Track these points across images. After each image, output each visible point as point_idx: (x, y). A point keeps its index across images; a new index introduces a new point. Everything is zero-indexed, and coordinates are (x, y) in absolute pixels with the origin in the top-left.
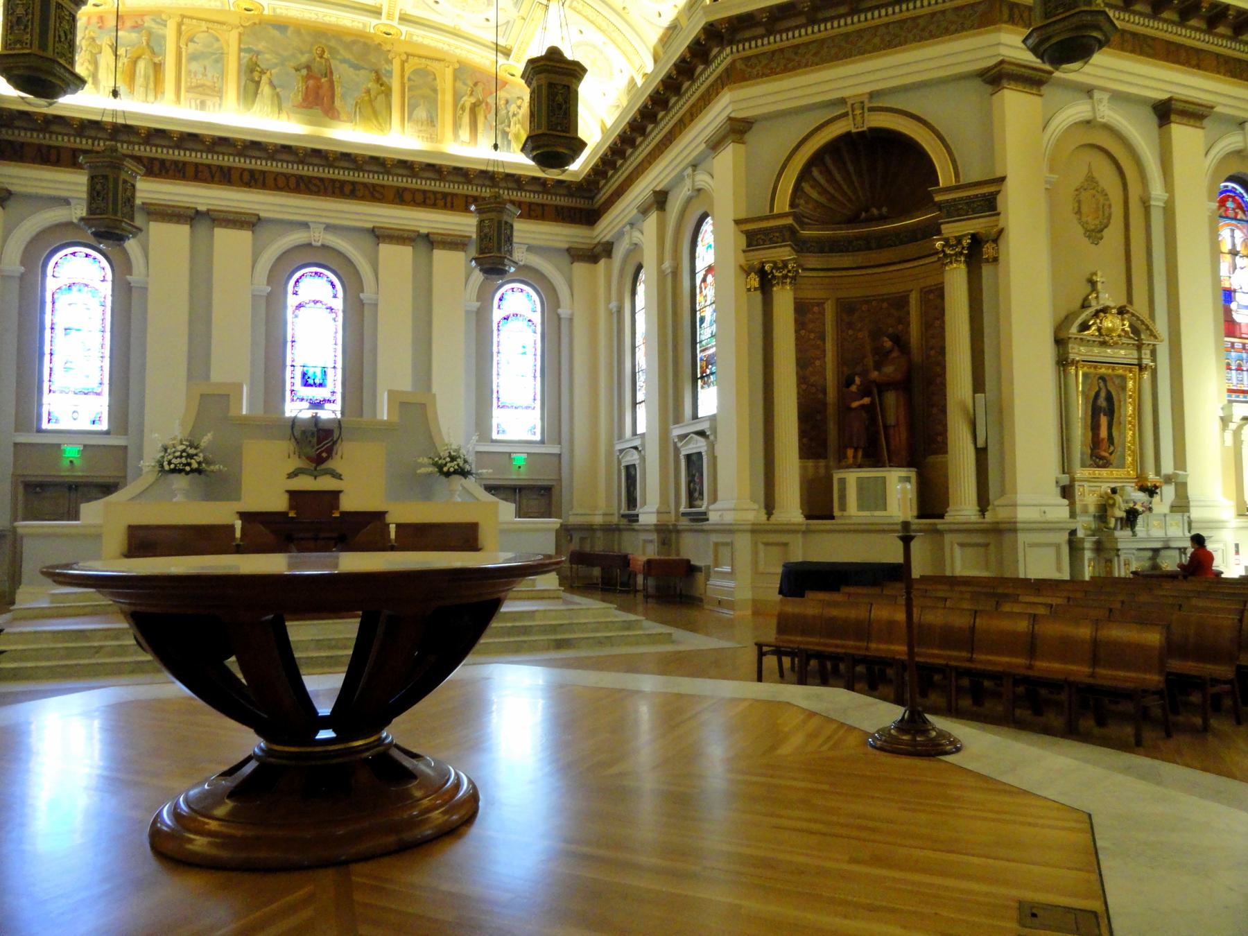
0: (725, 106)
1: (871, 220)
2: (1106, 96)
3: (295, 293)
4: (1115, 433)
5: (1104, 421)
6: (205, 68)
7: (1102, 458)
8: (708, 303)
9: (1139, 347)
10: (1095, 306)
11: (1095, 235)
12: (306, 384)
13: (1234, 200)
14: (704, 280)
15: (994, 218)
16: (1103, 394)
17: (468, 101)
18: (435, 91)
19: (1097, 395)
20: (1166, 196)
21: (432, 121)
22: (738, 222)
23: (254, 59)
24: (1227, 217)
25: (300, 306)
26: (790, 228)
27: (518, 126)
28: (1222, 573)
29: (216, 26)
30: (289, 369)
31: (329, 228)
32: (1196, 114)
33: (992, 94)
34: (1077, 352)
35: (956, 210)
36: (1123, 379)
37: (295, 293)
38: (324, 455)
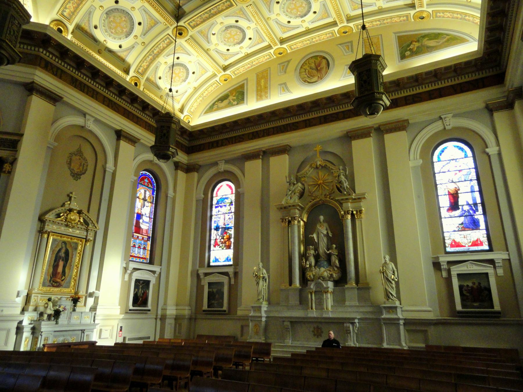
2: (93, 119)
4: (67, 270)
5: (61, 263)
7: (56, 282)
9: (87, 231)
10: (67, 206)
11: (76, 176)
13: (148, 179)
15: (14, 152)
16: (63, 251)
19: (60, 251)
20: (114, 168)
24: (144, 185)
28: (96, 342)
32: (133, 140)
33: (28, 96)
34: (49, 227)
36: (77, 244)
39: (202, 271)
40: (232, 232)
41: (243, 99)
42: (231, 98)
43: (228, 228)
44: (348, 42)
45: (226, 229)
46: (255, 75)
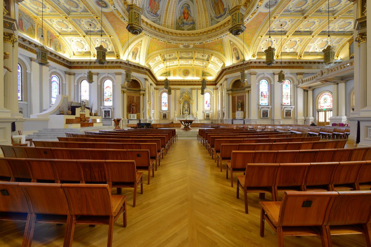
0: (225, 77)
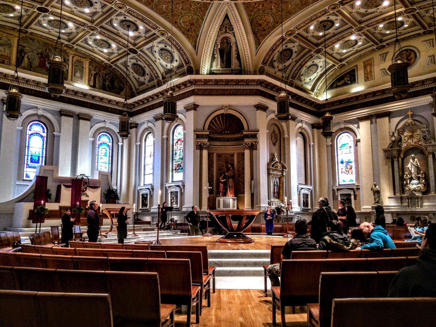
1: (225, 134)
3: (30, 130)
6: (5, 49)
8: (178, 149)
12: (32, 161)
14: (177, 142)
16: (276, 181)
17: (93, 72)
18: (83, 68)
21: (81, 78)
22: (194, 131)
23: (23, 48)
25: (32, 134)
26: (208, 135)
27: (109, 83)
29: (9, 35)
30: (26, 156)
31: (44, 110)
35: (247, 136)
37: (30, 130)
38: (85, 190)
39: (335, 188)
40: (353, 164)
41: (355, 80)
42: (346, 79)
43: (351, 162)
44: (431, 40)
45: (348, 162)
46: (363, 63)
